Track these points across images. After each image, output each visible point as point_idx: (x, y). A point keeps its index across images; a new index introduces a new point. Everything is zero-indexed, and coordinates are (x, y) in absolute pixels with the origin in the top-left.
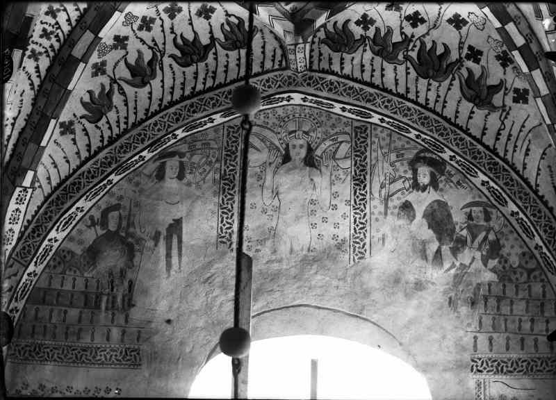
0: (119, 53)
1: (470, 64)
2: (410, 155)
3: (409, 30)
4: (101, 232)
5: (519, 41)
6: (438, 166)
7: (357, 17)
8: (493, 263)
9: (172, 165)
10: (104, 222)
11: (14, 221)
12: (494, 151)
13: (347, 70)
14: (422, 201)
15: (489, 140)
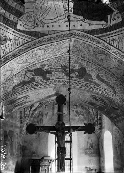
2: (74, 105)
4: (39, 114)
6: (77, 106)
9: (47, 106)
10: (39, 113)
14: (75, 110)
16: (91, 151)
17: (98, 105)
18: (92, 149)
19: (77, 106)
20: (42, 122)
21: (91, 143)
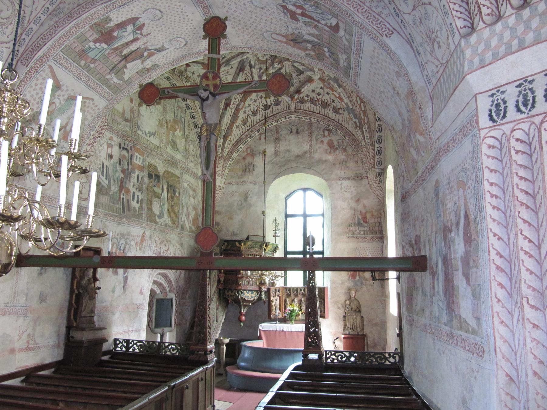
0: (249, 108)
1: (333, 103)
2: (323, 129)
3: (318, 97)
4: (246, 154)
5: (338, 96)
6: (330, 131)
7: (305, 95)
8: (344, 154)
11: (226, 148)
12: (342, 125)
13: (305, 109)
14: (326, 140)
15: (340, 122)
16: (363, 229)
17: (307, 41)
18: (366, 225)
19: (330, 131)
20: (254, 170)
21: (363, 211)
